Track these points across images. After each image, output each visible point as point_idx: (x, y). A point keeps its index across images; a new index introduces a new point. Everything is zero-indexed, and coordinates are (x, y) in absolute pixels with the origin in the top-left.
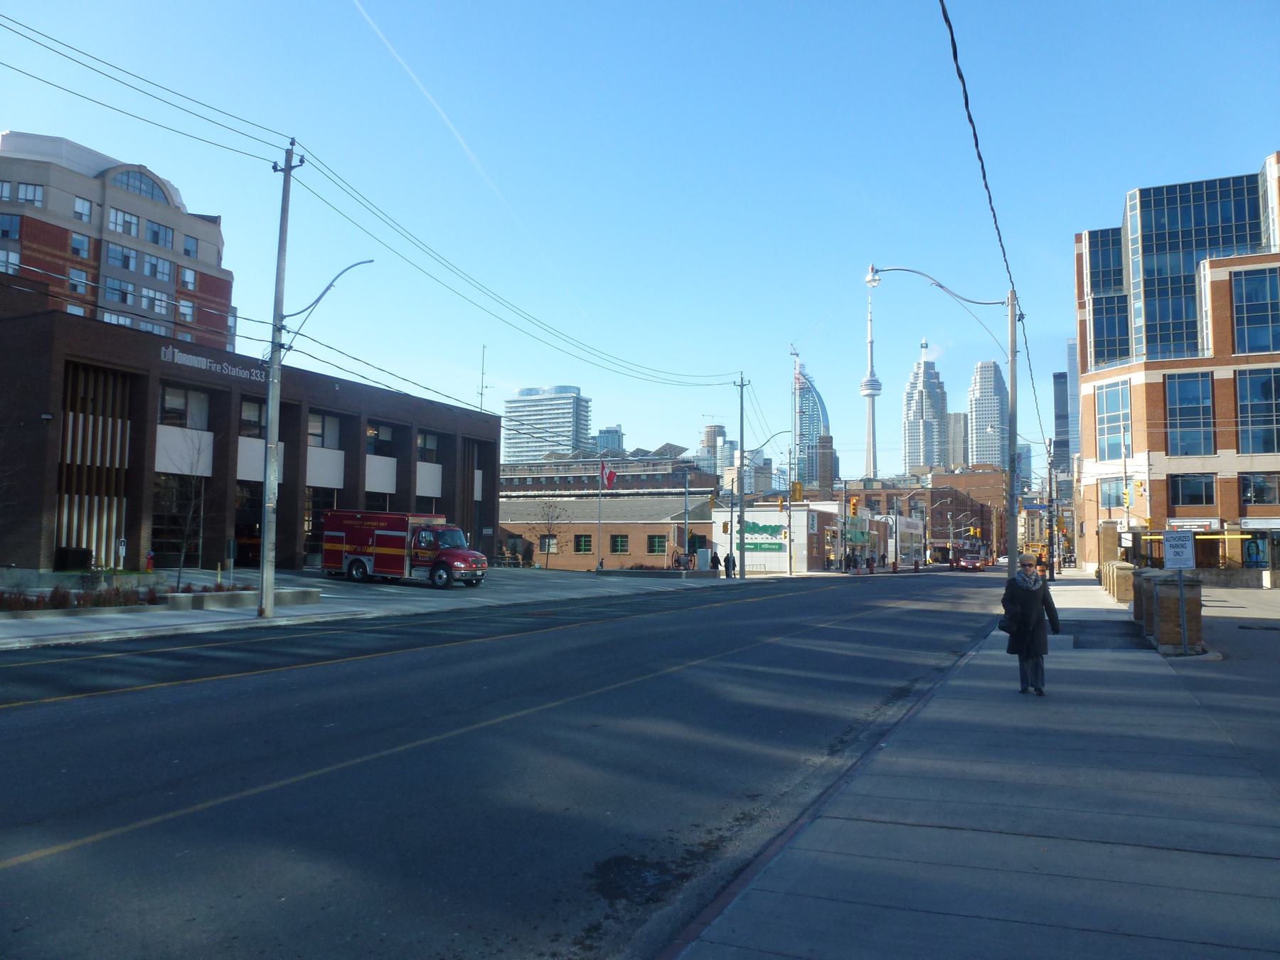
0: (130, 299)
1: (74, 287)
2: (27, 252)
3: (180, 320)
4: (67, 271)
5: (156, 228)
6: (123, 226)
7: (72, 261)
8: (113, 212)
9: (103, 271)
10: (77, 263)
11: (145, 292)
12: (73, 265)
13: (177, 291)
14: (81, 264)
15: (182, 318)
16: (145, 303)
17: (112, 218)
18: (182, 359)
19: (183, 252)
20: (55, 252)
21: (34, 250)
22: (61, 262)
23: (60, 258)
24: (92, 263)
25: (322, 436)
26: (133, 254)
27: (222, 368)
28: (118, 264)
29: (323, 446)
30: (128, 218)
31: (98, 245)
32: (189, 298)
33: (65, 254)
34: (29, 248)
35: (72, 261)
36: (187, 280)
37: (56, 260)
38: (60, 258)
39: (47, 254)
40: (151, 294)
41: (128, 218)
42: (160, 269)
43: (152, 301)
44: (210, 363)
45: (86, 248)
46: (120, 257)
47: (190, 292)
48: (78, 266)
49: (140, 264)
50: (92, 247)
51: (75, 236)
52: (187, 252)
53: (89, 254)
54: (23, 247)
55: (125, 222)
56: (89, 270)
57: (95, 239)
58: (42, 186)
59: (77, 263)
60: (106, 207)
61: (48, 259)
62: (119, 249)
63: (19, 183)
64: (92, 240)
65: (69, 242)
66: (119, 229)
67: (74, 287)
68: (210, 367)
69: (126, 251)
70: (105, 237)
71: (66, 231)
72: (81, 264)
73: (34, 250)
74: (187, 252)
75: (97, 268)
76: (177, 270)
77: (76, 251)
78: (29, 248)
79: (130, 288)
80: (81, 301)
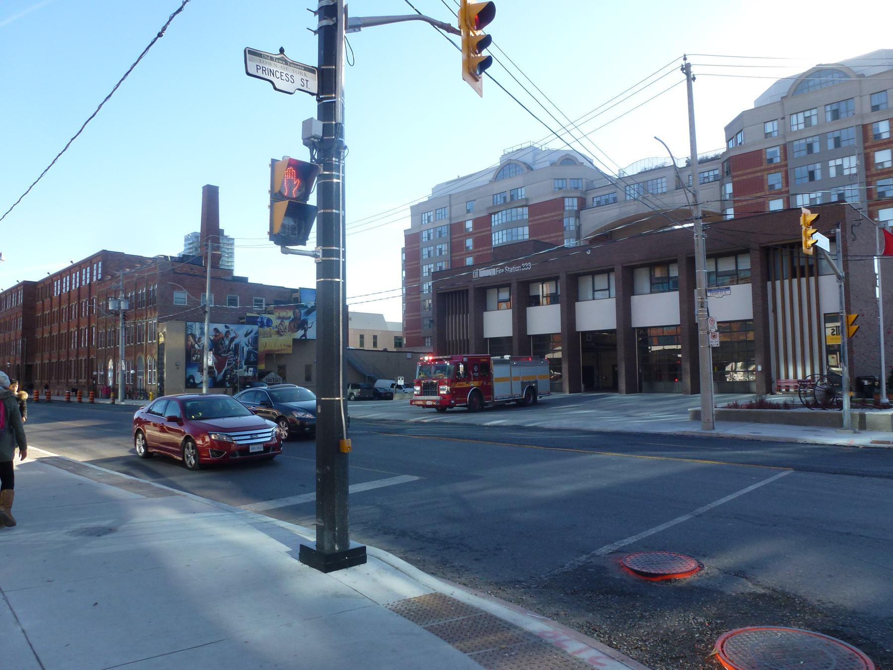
0: (818, 175)
1: (772, 187)
2: (736, 179)
3: (877, 170)
4: (765, 178)
5: (834, 107)
6: (805, 123)
7: (768, 169)
8: (794, 117)
9: (789, 167)
10: (771, 169)
11: (832, 163)
12: (769, 172)
13: (865, 148)
14: (775, 168)
15: (880, 167)
16: (833, 172)
17: (794, 122)
18: (484, 273)
19: (870, 110)
20: (754, 169)
21: (740, 175)
22: (759, 174)
23: (758, 171)
24: (783, 163)
25: (609, 289)
26: (817, 139)
27: (505, 270)
28: (804, 153)
29: (610, 298)
30: (807, 114)
31: (784, 148)
32: (884, 147)
33: (762, 167)
34: (737, 176)
35: (768, 169)
36: (880, 132)
37: (756, 175)
38: (758, 171)
39: (749, 173)
40: (839, 162)
41: (807, 114)
42: (844, 137)
43: (839, 168)
44: (498, 270)
45: (779, 154)
46: (805, 147)
47: (885, 141)
48: (773, 171)
49: (823, 144)
50: (782, 151)
51: (769, 150)
52: (875, 108)
53: (780, 158)
54: (733, 177)
55: (805, 118)
56: (781, 169)
57: (784, 144)
58: (776, 120)
59: (771, 169)
60: (787, 117)
61: (750, 176)
62: (803, 141)
63: (737, 134)
64: (782, 146)
65: (764, 157)
66: (802, 127)
67: (772, 187)
68: (498, 272)
69: (809, 140)
70: (789, 139)
71: (759, 153)
72: (775, 168)
73: (740, 175)
74: (875, 108)
75: (786, 165)
76: (865, 129)
77: (771, 161)
78: (737, 176)
79: (818, 166)
80: (777, 195)
